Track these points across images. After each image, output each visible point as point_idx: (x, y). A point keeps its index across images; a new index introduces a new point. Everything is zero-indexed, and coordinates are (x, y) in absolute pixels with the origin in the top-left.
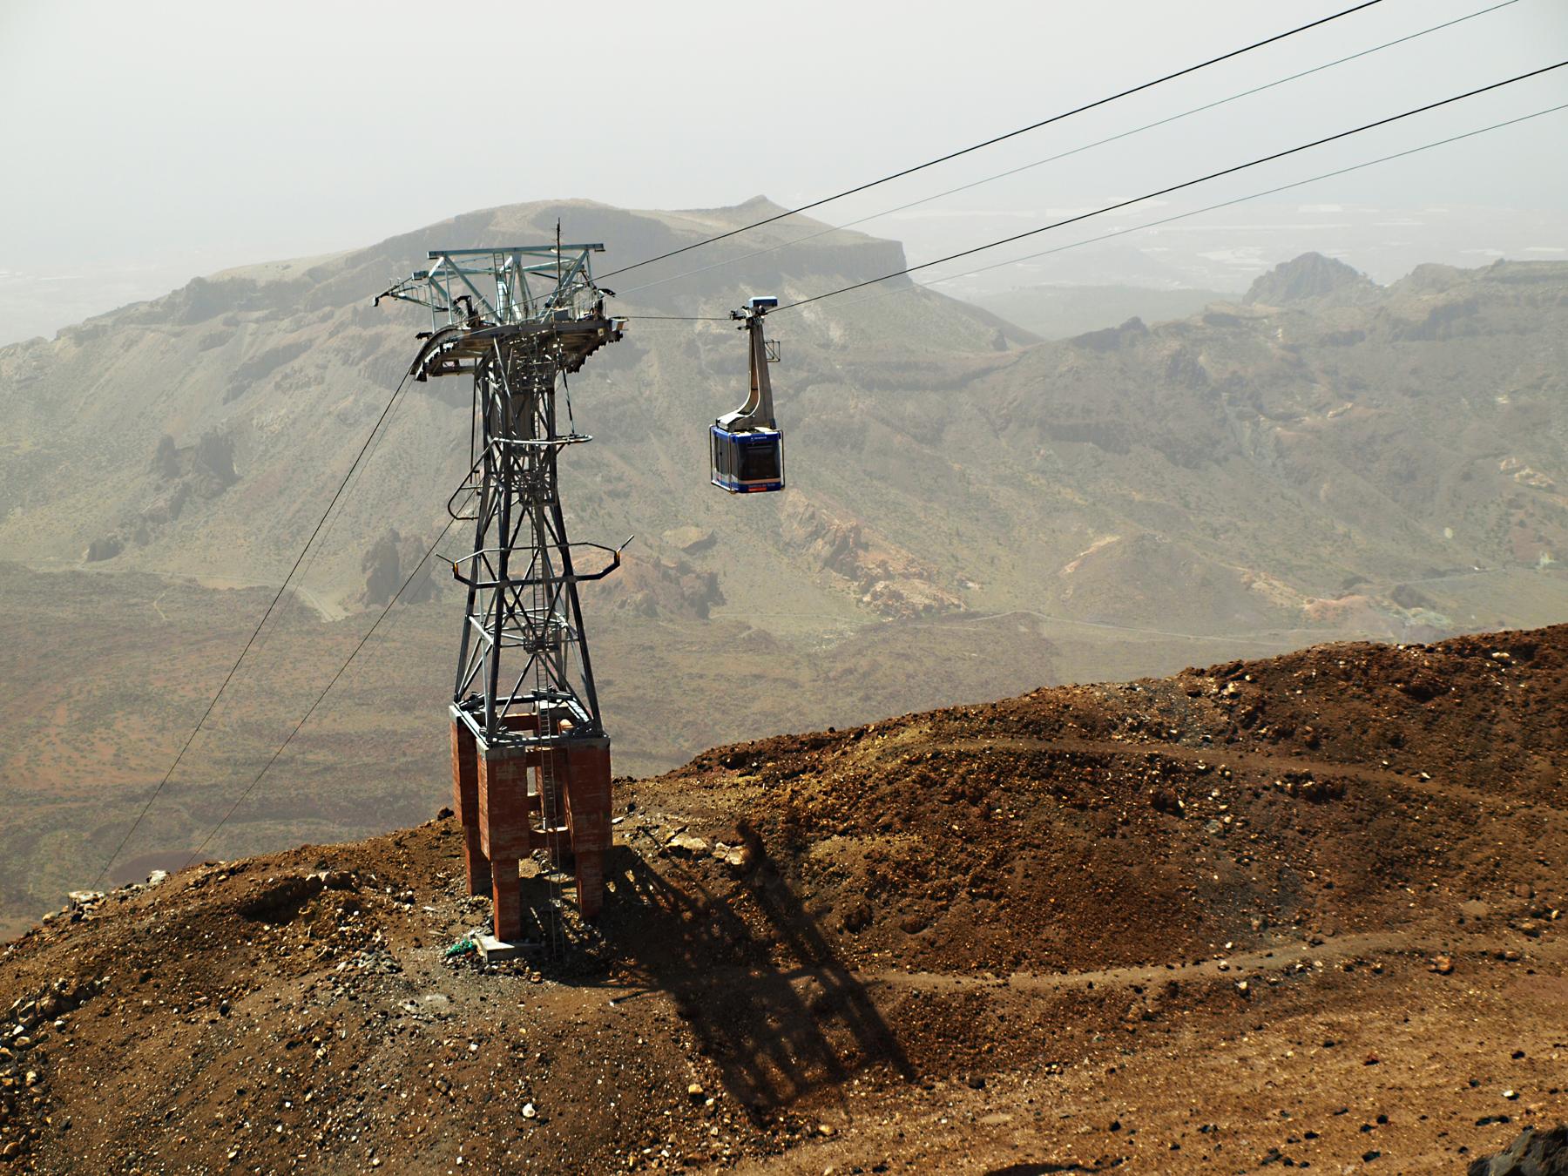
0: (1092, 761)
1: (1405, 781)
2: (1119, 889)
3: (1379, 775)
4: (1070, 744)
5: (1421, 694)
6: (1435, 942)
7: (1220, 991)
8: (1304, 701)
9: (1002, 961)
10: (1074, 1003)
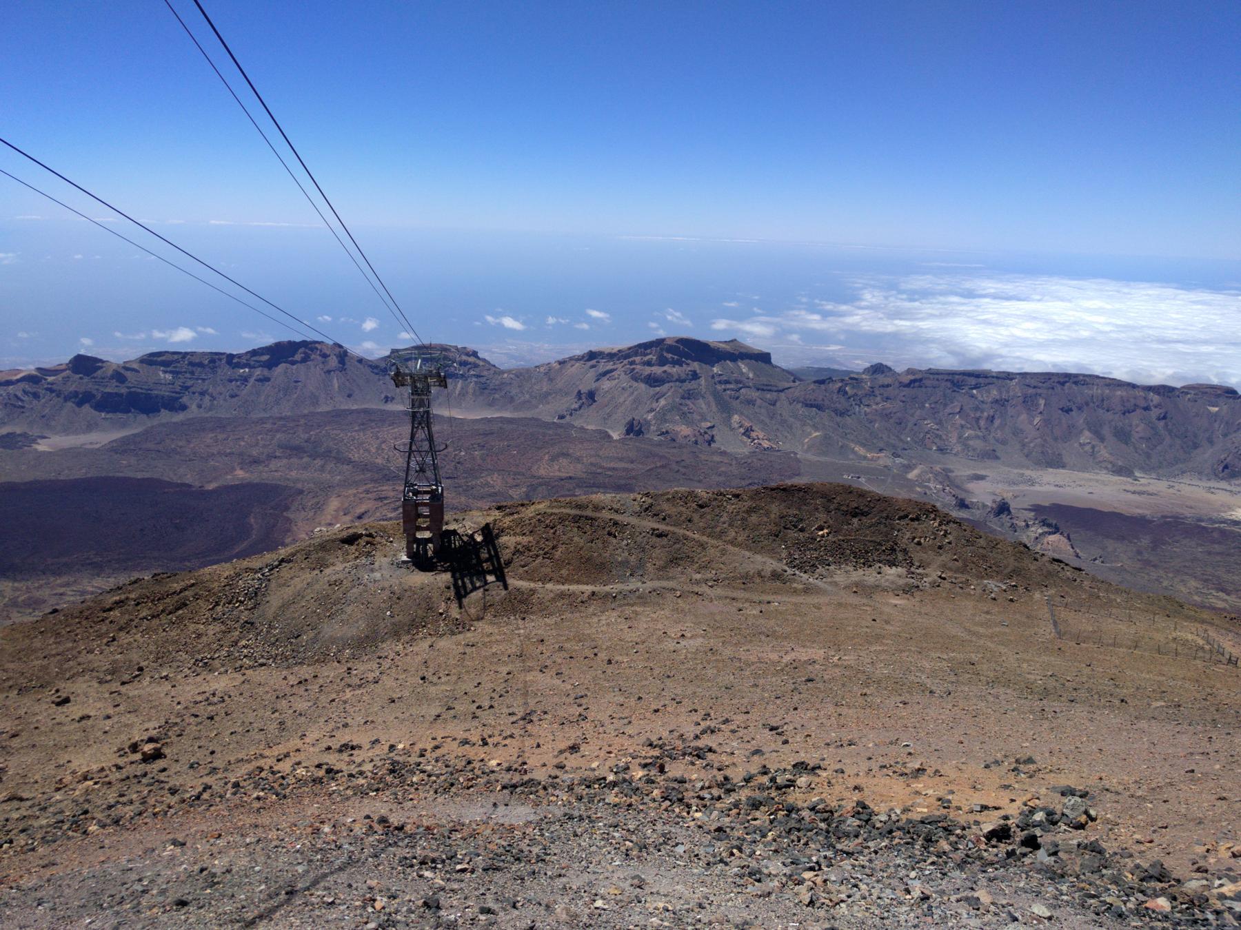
0: (592, 519)
1: (689, 533)
2: (588, 559)
3: (680, 531)
4: (589, 513)
5: (701, 506)
6: (678, 587)
7: (607, 595)
8: (665, 506)
9: (545, 579)
10: (562, 595)
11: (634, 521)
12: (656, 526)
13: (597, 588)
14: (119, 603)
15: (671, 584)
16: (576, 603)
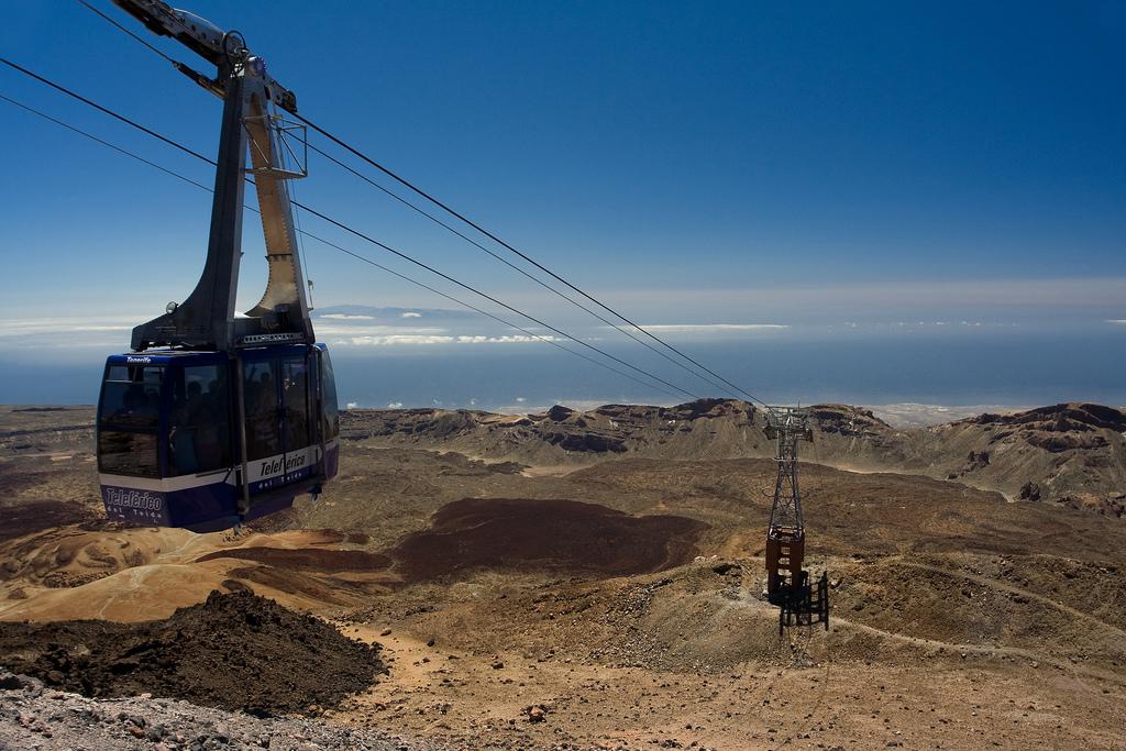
0: (945, 576)
1: (1054, 603)
4: (943, 570)
5: (1069, 576)
9: (893, 630)
10: (910, 647)
11: (990, 582)
12: (1015, 591)
13: (947, 646)
14: (545, 598)
15: (1029, 653)
16: (921, 656)
